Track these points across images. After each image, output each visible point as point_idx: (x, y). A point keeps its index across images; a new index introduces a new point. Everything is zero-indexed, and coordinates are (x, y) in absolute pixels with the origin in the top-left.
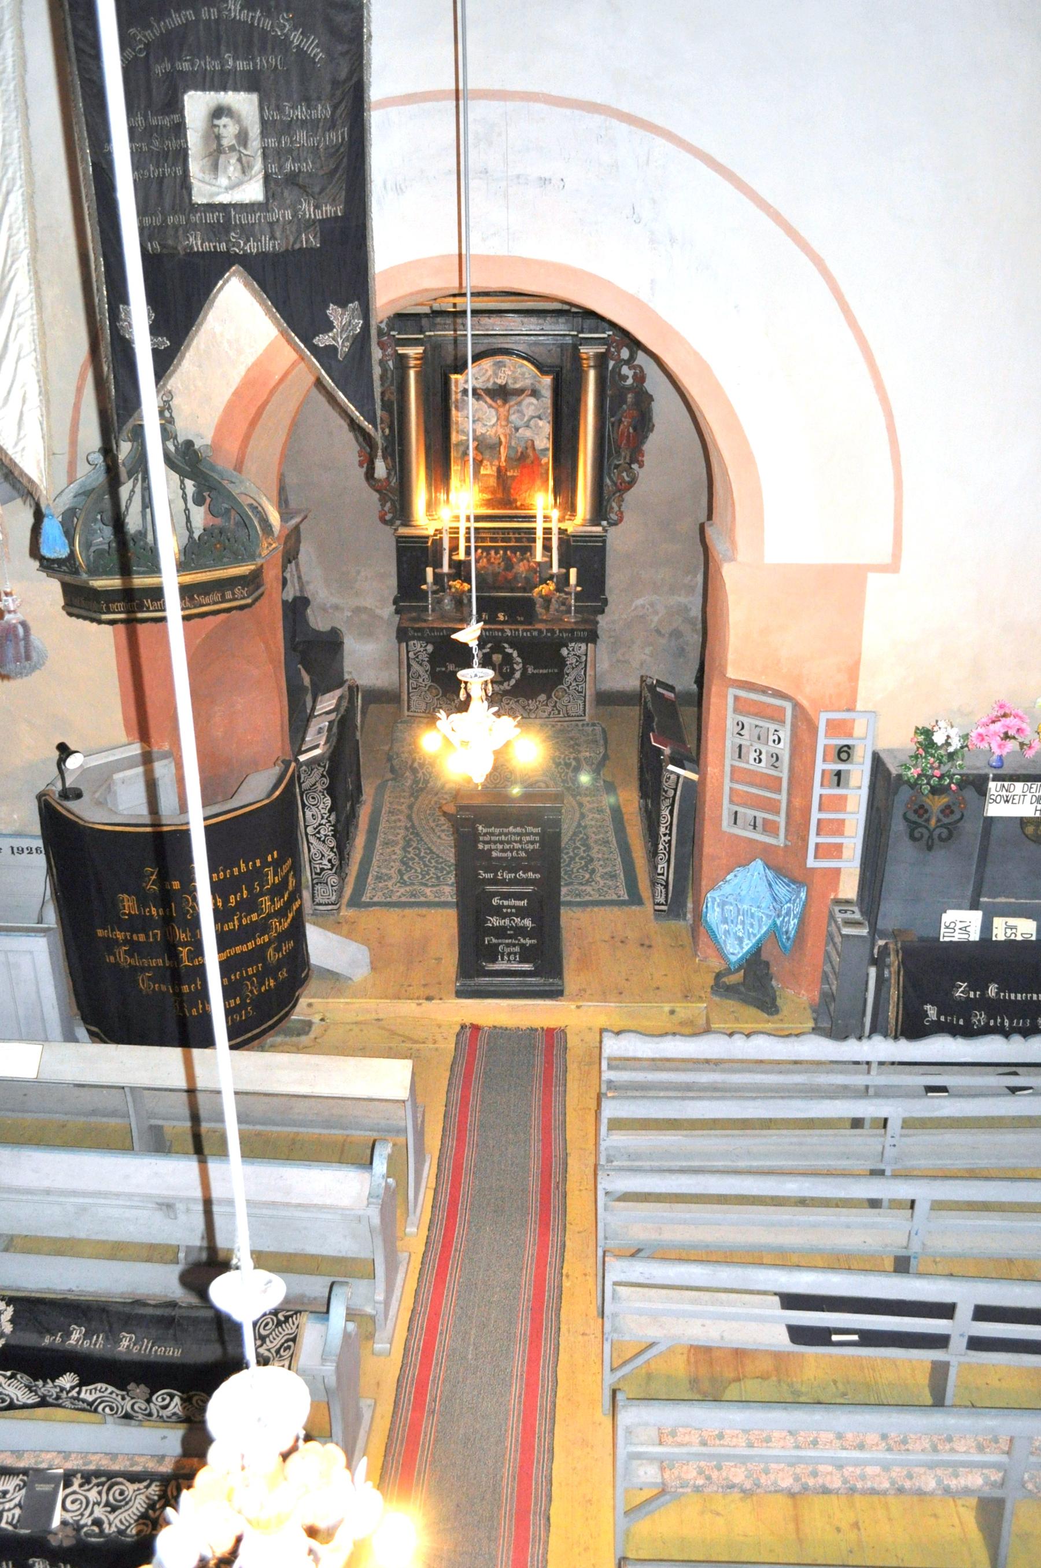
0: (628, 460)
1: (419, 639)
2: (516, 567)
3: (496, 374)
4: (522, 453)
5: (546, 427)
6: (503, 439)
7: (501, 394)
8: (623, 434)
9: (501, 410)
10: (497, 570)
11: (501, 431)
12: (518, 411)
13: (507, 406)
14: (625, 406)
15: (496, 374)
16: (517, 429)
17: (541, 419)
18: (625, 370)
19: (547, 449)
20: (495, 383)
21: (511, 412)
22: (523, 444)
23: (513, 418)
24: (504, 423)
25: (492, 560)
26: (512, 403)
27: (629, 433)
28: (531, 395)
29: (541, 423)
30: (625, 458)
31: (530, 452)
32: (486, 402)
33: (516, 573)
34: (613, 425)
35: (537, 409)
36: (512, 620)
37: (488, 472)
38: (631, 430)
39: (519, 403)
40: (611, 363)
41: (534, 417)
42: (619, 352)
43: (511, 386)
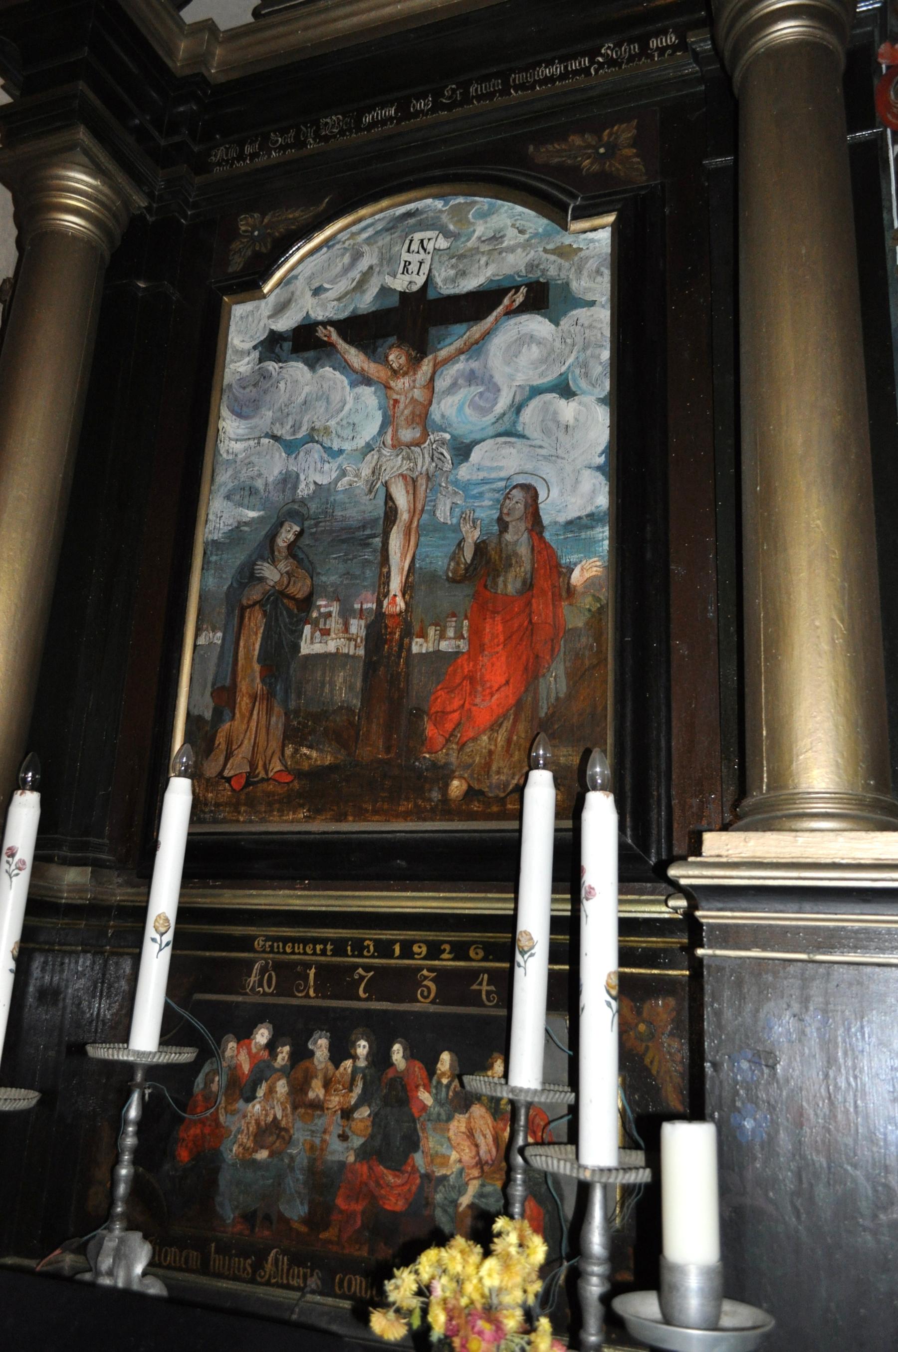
2: (430, 1141)
3: (388, 260)
4: (480, 548)
5: (590, 423)
6: (402, 499)
9: (401, 384)
10: (341, 1152)
12: (472, 378)
13: (426, 366)
15: (388, 260)
16: (462, 451)
17: (565, 390)
19: (593, 519)
20: (385, 290)
21: (441, 384)
22: (486, 512)
24: (407, 434)
25: (317, 1091)
26: (443, 354)
28: (526, 308)
29: (567, 410)
31: (518, 538)
32: (345, 367)
33: (427, 1177)
35: (547, 360)
37: (331, 646)
39: (475, 348)
41: (536, 391)
43: (447, 290)
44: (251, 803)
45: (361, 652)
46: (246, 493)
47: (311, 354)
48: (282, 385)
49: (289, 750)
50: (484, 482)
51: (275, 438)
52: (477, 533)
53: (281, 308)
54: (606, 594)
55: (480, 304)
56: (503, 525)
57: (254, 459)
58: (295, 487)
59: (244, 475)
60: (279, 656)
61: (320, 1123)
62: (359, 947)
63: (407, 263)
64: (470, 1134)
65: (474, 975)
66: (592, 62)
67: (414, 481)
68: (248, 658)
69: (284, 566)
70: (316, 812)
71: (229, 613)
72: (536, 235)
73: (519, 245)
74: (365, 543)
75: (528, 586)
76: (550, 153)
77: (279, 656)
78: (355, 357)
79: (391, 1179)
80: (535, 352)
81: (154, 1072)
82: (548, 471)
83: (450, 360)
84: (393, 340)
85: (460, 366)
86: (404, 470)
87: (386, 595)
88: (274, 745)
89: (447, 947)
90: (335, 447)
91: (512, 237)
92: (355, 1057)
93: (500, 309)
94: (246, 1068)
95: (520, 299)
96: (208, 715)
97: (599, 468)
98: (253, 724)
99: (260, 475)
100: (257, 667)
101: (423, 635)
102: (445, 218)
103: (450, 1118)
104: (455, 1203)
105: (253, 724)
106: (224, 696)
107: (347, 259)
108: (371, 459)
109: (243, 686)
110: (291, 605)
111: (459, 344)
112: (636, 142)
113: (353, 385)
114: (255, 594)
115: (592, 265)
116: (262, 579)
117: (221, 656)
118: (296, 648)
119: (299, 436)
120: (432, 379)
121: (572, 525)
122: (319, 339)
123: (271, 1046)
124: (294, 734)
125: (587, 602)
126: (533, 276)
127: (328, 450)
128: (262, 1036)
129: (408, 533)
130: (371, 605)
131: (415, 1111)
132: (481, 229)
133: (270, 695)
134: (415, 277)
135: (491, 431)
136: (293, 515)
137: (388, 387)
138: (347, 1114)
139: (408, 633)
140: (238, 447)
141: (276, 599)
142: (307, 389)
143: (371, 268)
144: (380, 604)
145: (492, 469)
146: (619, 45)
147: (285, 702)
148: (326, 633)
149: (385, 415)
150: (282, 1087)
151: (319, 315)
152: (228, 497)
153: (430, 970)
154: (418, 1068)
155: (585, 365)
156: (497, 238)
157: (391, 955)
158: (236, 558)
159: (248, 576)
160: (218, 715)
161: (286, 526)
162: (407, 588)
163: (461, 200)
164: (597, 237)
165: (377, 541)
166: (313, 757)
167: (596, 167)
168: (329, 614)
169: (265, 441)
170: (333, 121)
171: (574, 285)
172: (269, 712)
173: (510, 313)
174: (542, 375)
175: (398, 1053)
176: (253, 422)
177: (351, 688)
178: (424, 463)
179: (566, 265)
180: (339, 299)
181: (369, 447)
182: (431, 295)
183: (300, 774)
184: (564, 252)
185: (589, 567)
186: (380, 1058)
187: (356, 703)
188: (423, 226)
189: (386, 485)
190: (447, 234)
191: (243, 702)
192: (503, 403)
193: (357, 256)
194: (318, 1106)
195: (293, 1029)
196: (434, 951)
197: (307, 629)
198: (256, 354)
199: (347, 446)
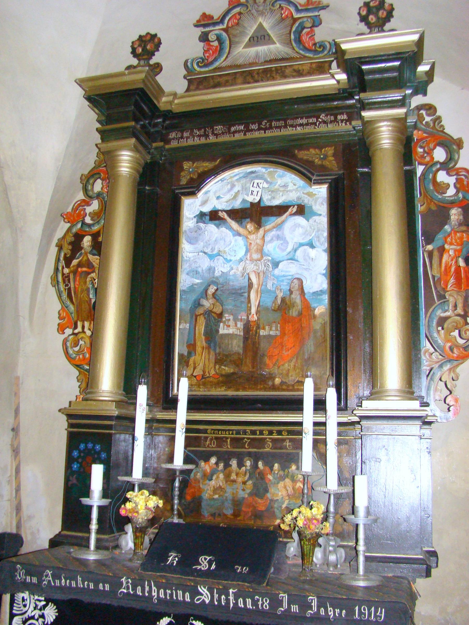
0: (460, 310)
1: (34, 589)
2: (272, 490)
4: (283, 300)
5: (320, 259)
6: (254, 280)
7: (254, 214)
8: (448, 268)
9: (252, 237)
11: (251, 267)
12: (278, 238)
13: (261, 231)
14: (447, 227)
15: (245, 188)
16: (276, 264)
17: (312, 246)
18: (442, 177)
20: (244, 201)
21: (267, 239)
22: (285, 287)
23: (270, 248)
24: (255, 256)
25: (233, 476)
26: (267, 227)
27: (458, 268)
29: (312, 253)
30: (455, 306)
31: (296, 297)
32: (230, 228)
33: (272, 500)
34: (430, 254)
35: (305, 233)
36: (223, 571)
37: (231, 331)
38: (462, 263)
39: (279, 226)
40: (420, 169)
41: (301, 245)
42: (430, 153)
44: (204, 384)
45: (242, 334)
46: (195, 273)
47: (217, 222)
48: (206, 233)
49: (217, 367)
50: (284, 276)
51: (205, 253)
52: (282, 294)
53: (204, 203)
54: (327, 319)
55: (280, 210)
56: (291, 292)
57: (197, 260)
58: (214, 272)
59: (194, 266)
60: (211, 335)
61: (235, 486)
62: (245, 432)
63: (252, 191)
64: (285, 487)
65: (284, 440)
66: (317, 121)
67: (259, 274)
68: (200, 333)
69: (212, 301)
70: (229, 388)
71: (191, 317)
72: (300, 187)
73: (294, 190)
74: (241, 295)
75: (300, 314)
76: (302, 154)
77: (211, 335)
78: (234, 224)
79: (260, 501)
80: (300, 230)
81: (183, 472)
82: (305, 273)
83: (269, 230)
84: (248, 220)
85: (274, 233)
86: (255, 269)
87: (250, 314)
88: (212, 365)
89: (275, 432)
90: (228, 259)
91: (291, 187)
92: (246, 466)
93: (288, 213)
94: (208, 471)
95: (295, 210)
96: (186, 354)
97: (323, 274)
98: (203, 357)
99: (200, 267)
100: (203, 337)
101: (264, 329)
102: (266, 176)
103: (278, 483)
104: (281, 507)
105: (203, 357)
106: (192, 347)
107: (229, 187)
108: (242, 264)
109: (198, 344)
110: (214, 315)
111: (273, 224)
112: (334, 155)
113: (234, 235)
114: (201, 311)
115: (320, 201)
116: (203, 306)
117: (189, 333)
118: (217, 331)
119: (214, 253)
120: (264, 237)
121: (315, 294)
122: (220, 217)
123: (217, 464)
124: (219, 361)
125: (320, 320)
126: (299, 202)
127: (226, 259)
128: (213, 460)
129: (257, 292)
130: (244, 317)
131: (267, 482)
132: (280, 182)
133: (209, 348)
134: (255, 197)
135: (286, 258)
136: (214, 283)
137: (247, 238)
138: (244, 483)
139: (258, 328)
140: (191, 255)
141: (208, 313)
142: (216, 235)
143: (239, 191)
144: (248, 317)
145: (287, 272)
146: (327, 115)
147: (215, 350)
148: (229, 326)
149: (247, 248)
150: (221, 476)
151: (219, 207)
152: (188, 274)
153: (270, 438)
154: (267, 469)
155: (318, 237)
156: (285, 186)
157: (256, 434)
158: (193, 297)
159: (197, 304)
160: (190, 354)
161: (211, 286)
162: (258, 312)
163: (272, 170)
164: (322, 191)
165: (246, 295)
166: (227, 370)
167: (320, 163)
168: (229, 320)
169: (201, 254)
170: (219, 128)
171: (314, 208)
172: (209, 353)
173: (292, 215)
174: (303, 239)
175: (260, 464)
176: (196, 246)
177: (239, 346)
178: (262, 268)
179: (311, 199)
180: (227, 202)
181: (241, 260)
182: (262, 205)
183: (222, 375)
184: (310, 195)
185: (322, 308)
186: (255, 466)
187: (241, 351)
188: (257, 177)
189: (248, 274)
190: (267, 182)
191: (199, 349)
192: (290, 248)
193: (233, 186)
194: (234, 481)
195: (225, 458)
196: (271, 433)
197: (221, 325)
198: (195, 220)
199: (233, 258)
